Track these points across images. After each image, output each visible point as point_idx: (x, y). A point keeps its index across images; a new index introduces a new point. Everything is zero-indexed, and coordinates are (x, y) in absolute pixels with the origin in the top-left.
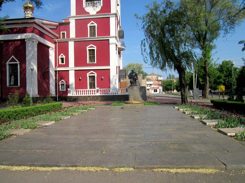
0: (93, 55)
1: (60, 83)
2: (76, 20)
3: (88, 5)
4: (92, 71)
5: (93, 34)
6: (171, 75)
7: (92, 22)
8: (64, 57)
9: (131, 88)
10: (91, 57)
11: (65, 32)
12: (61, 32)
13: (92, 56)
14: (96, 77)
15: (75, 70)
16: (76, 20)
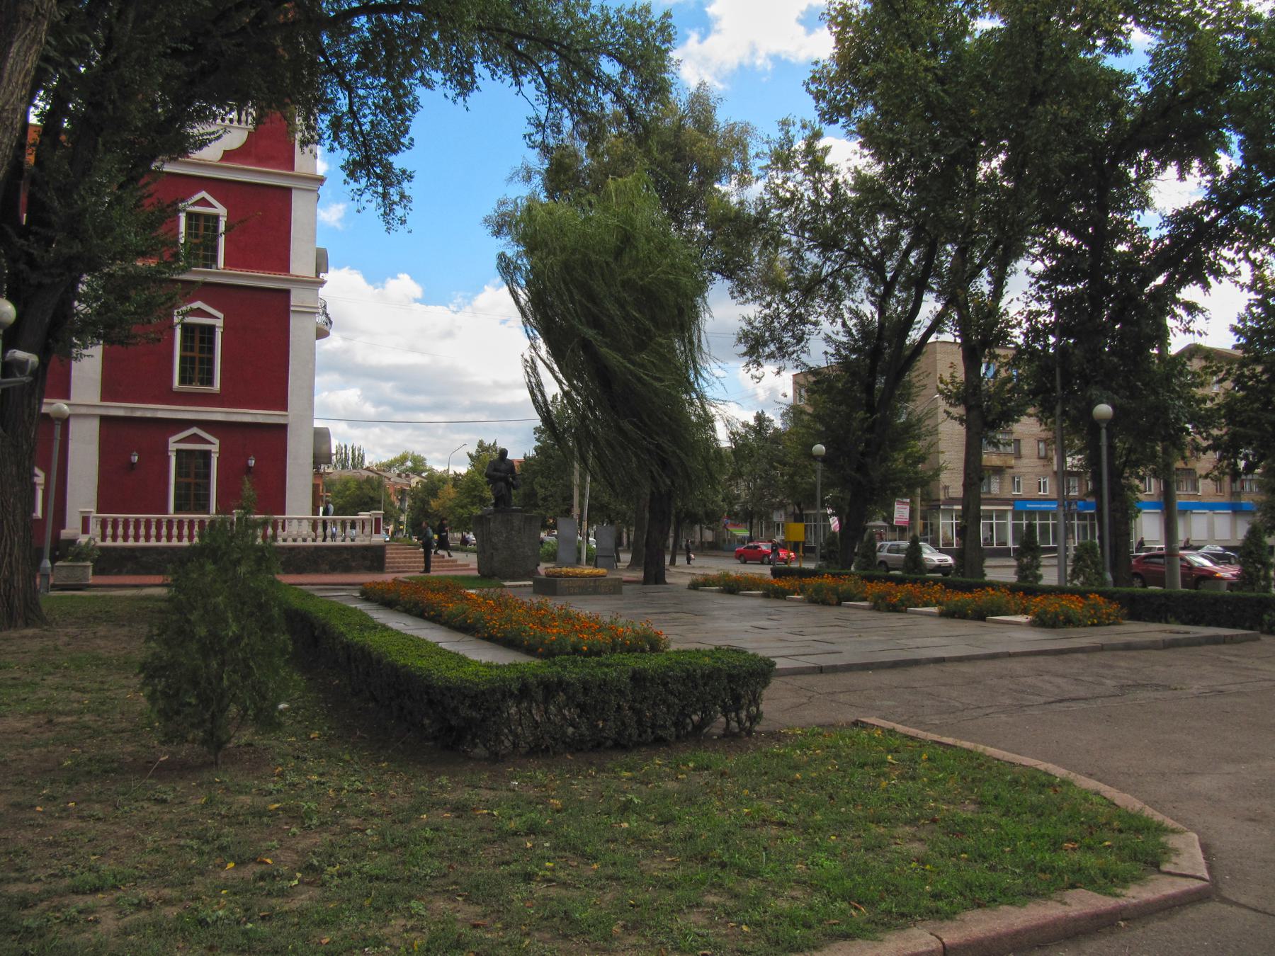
0: (202, 350)
4: (195, 430)
6: (349, 448)
7: (204, 194)
10: (192, 359)
13: (196, 354)
15: (104, 420)
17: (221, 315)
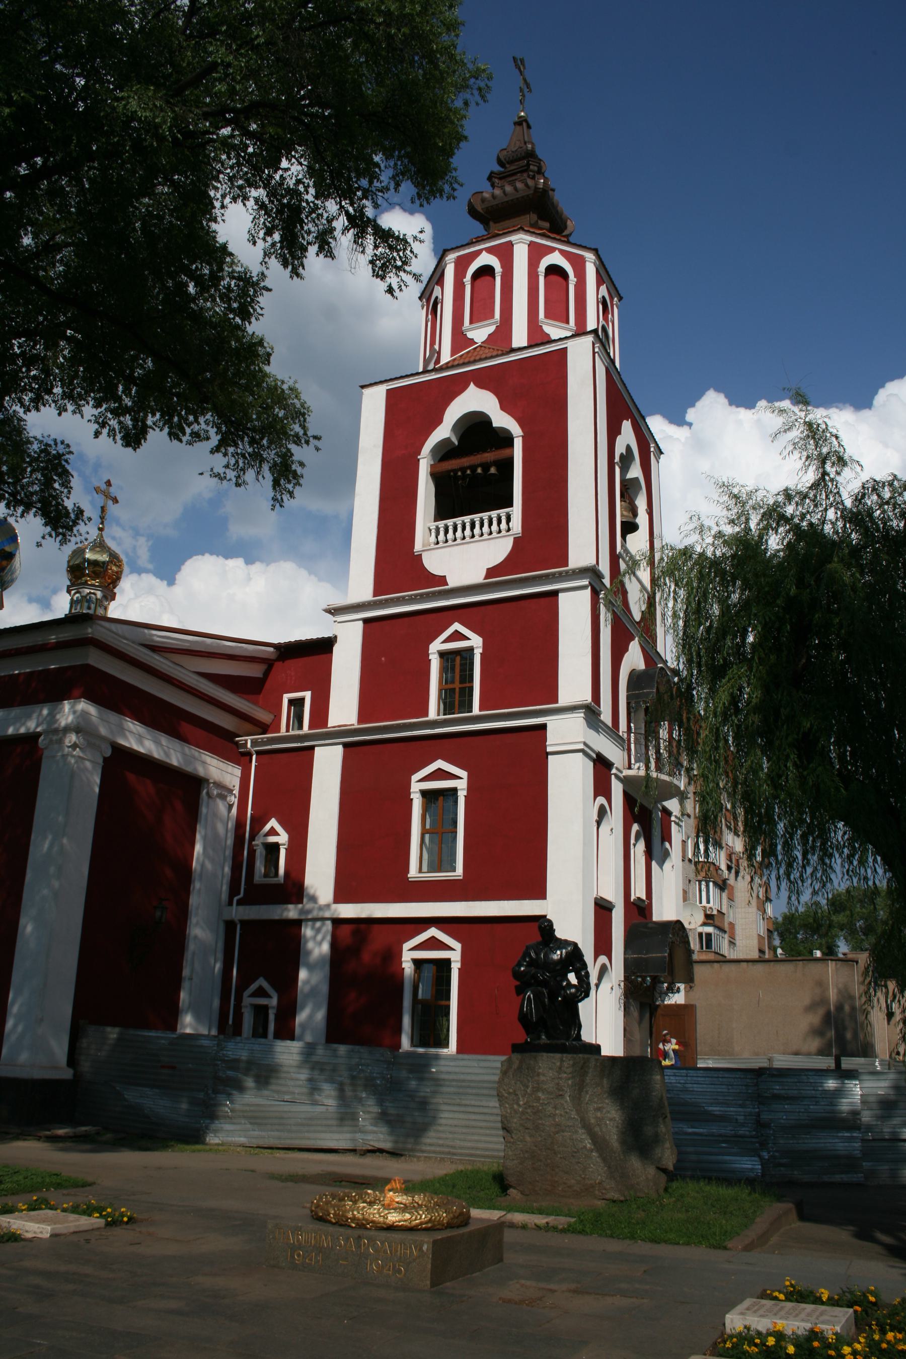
1: (248, 1001)
2: (366, 621)
3: (441, 537)
4: (433, 932)
5: (456, 698)
7: (457, 626)
8: (282, 838)
9: (520, 1068)
11: (307, 695)
12: (286, 697)
14: (455, 967)
16: (366, 621)
17: (463, 774)
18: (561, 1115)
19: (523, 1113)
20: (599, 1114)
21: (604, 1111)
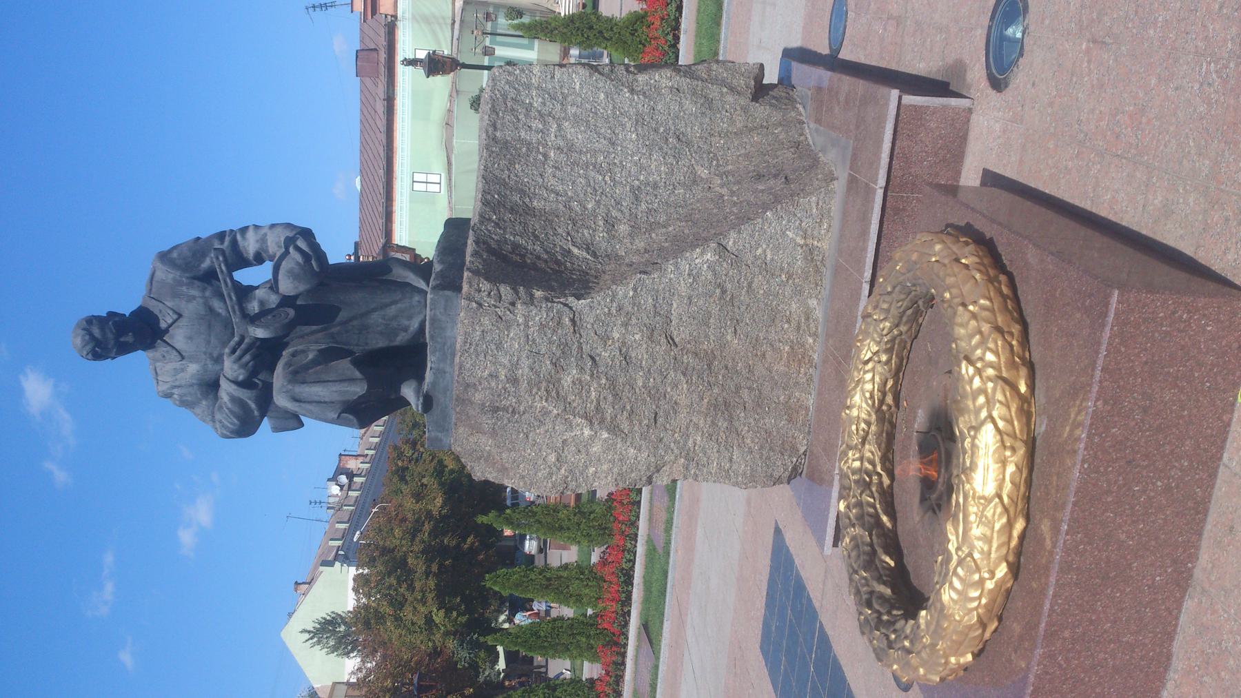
18: (625, 325)
19: (614, 429)
20: (623, 228)
21: (614, 213)
